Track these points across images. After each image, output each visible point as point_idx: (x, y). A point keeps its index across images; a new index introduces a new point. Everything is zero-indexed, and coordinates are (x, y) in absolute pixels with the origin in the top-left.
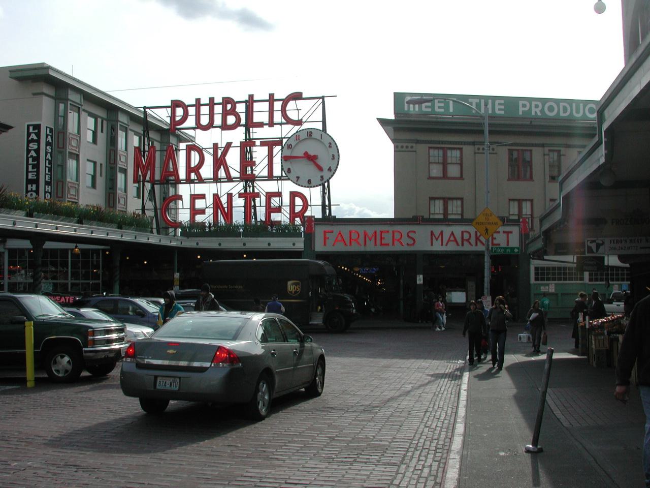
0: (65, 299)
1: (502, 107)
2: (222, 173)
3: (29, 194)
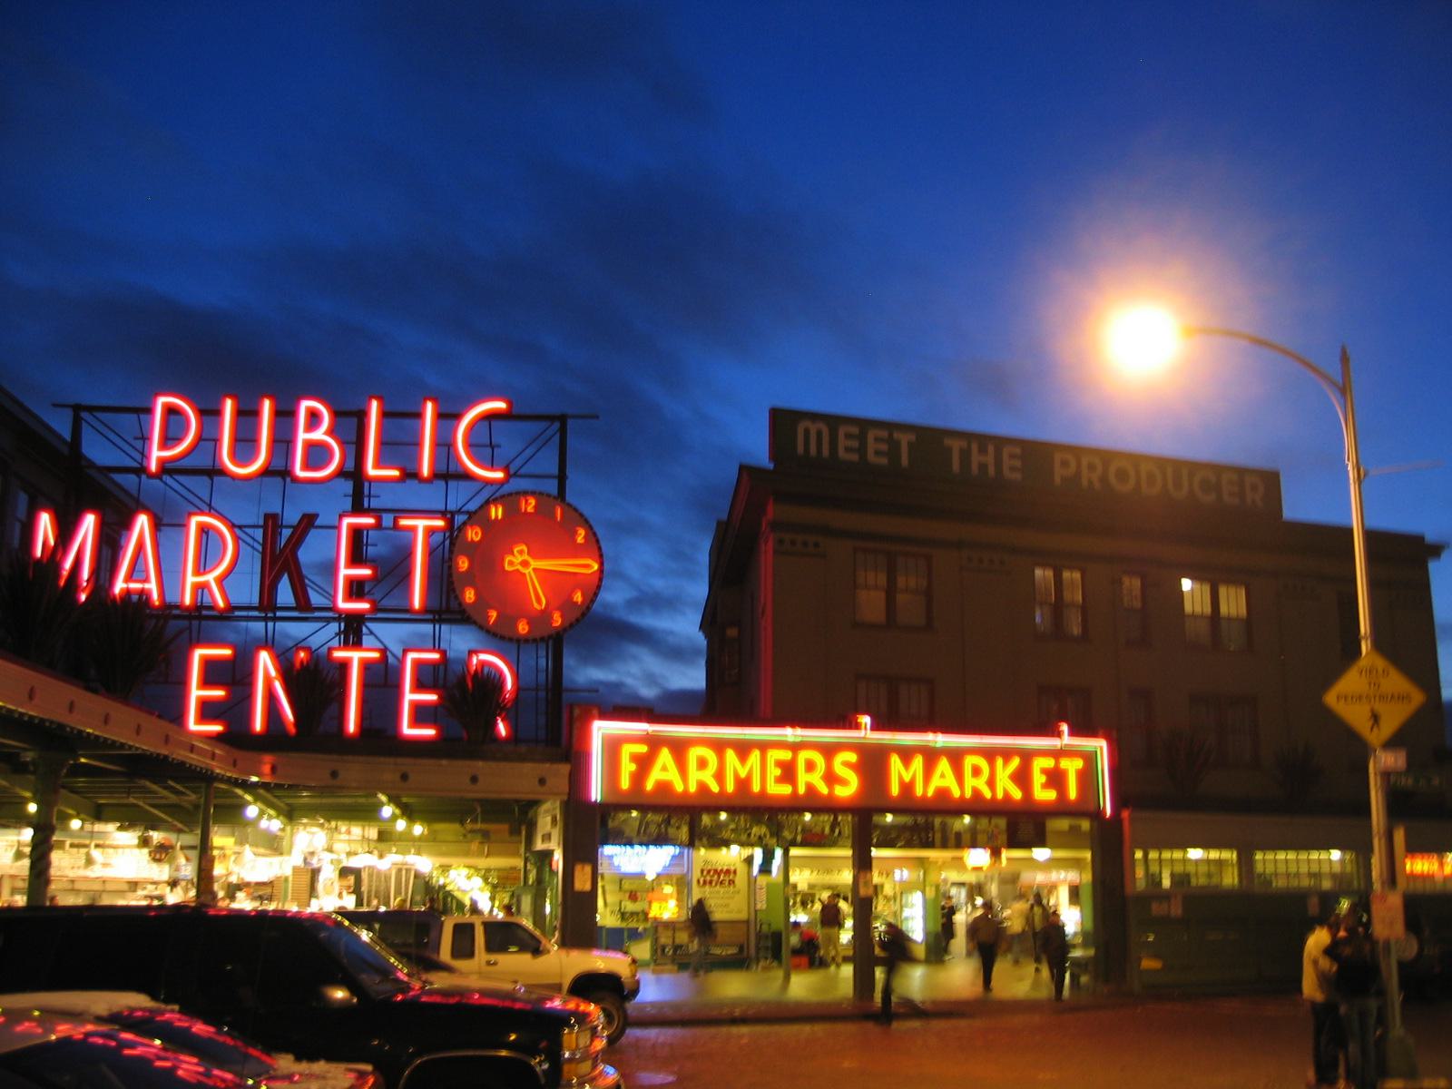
1: (1017, 463)
2: (285, 594)
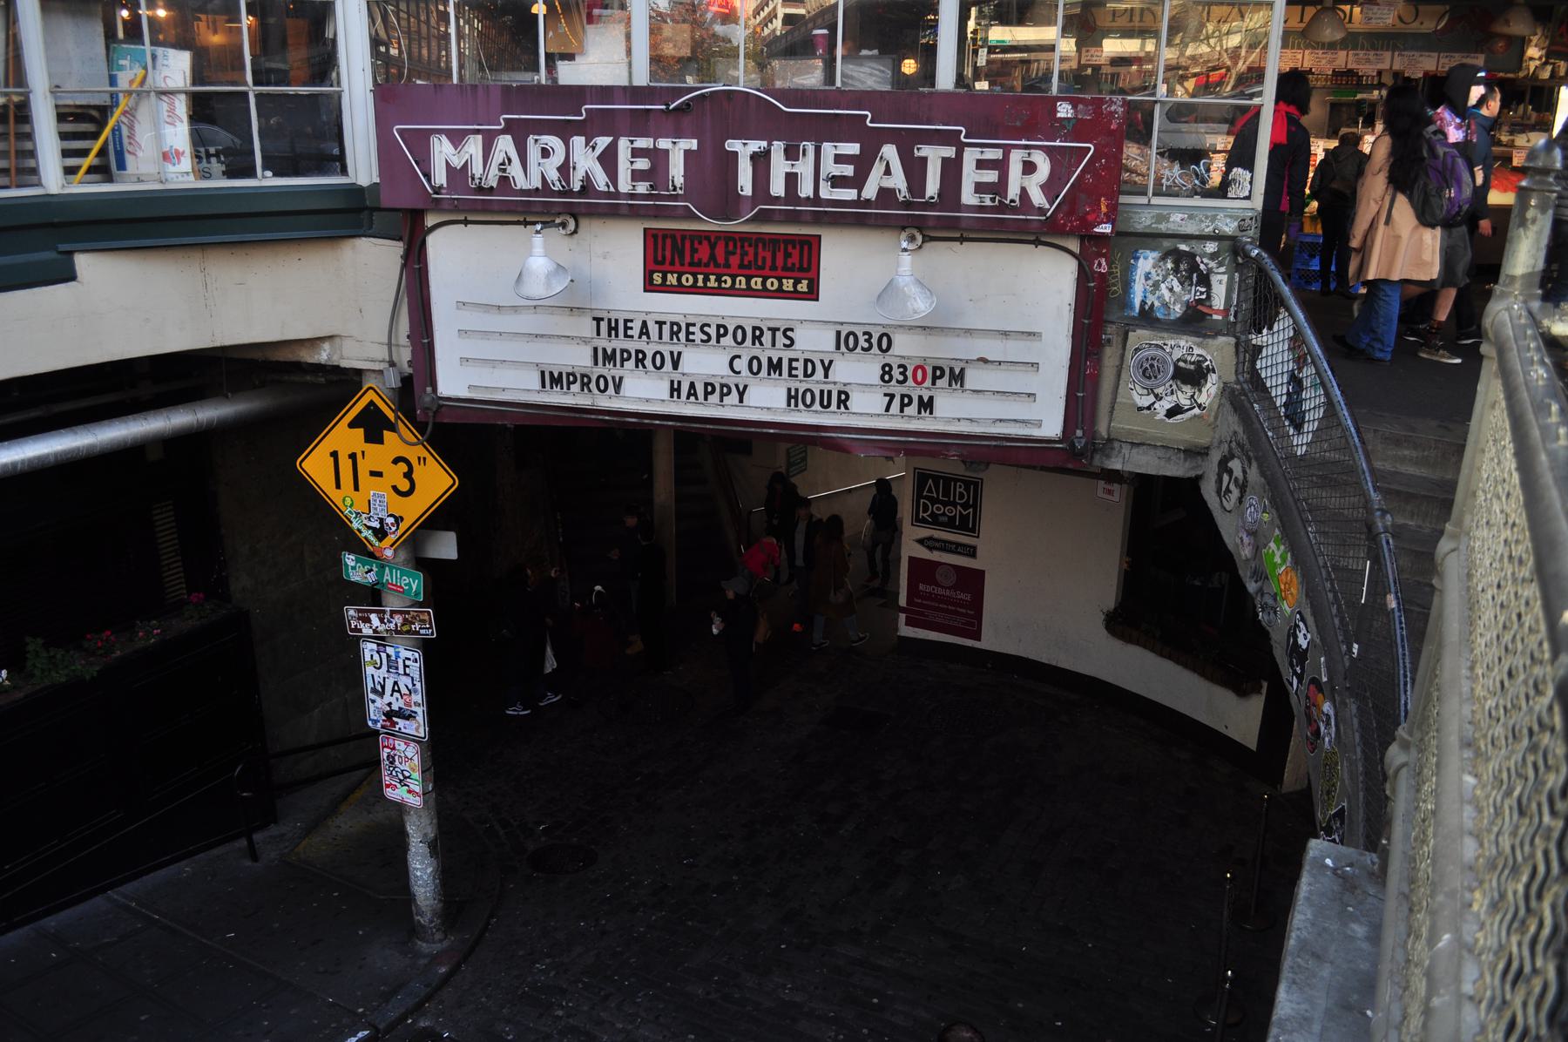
0: (915, 170)
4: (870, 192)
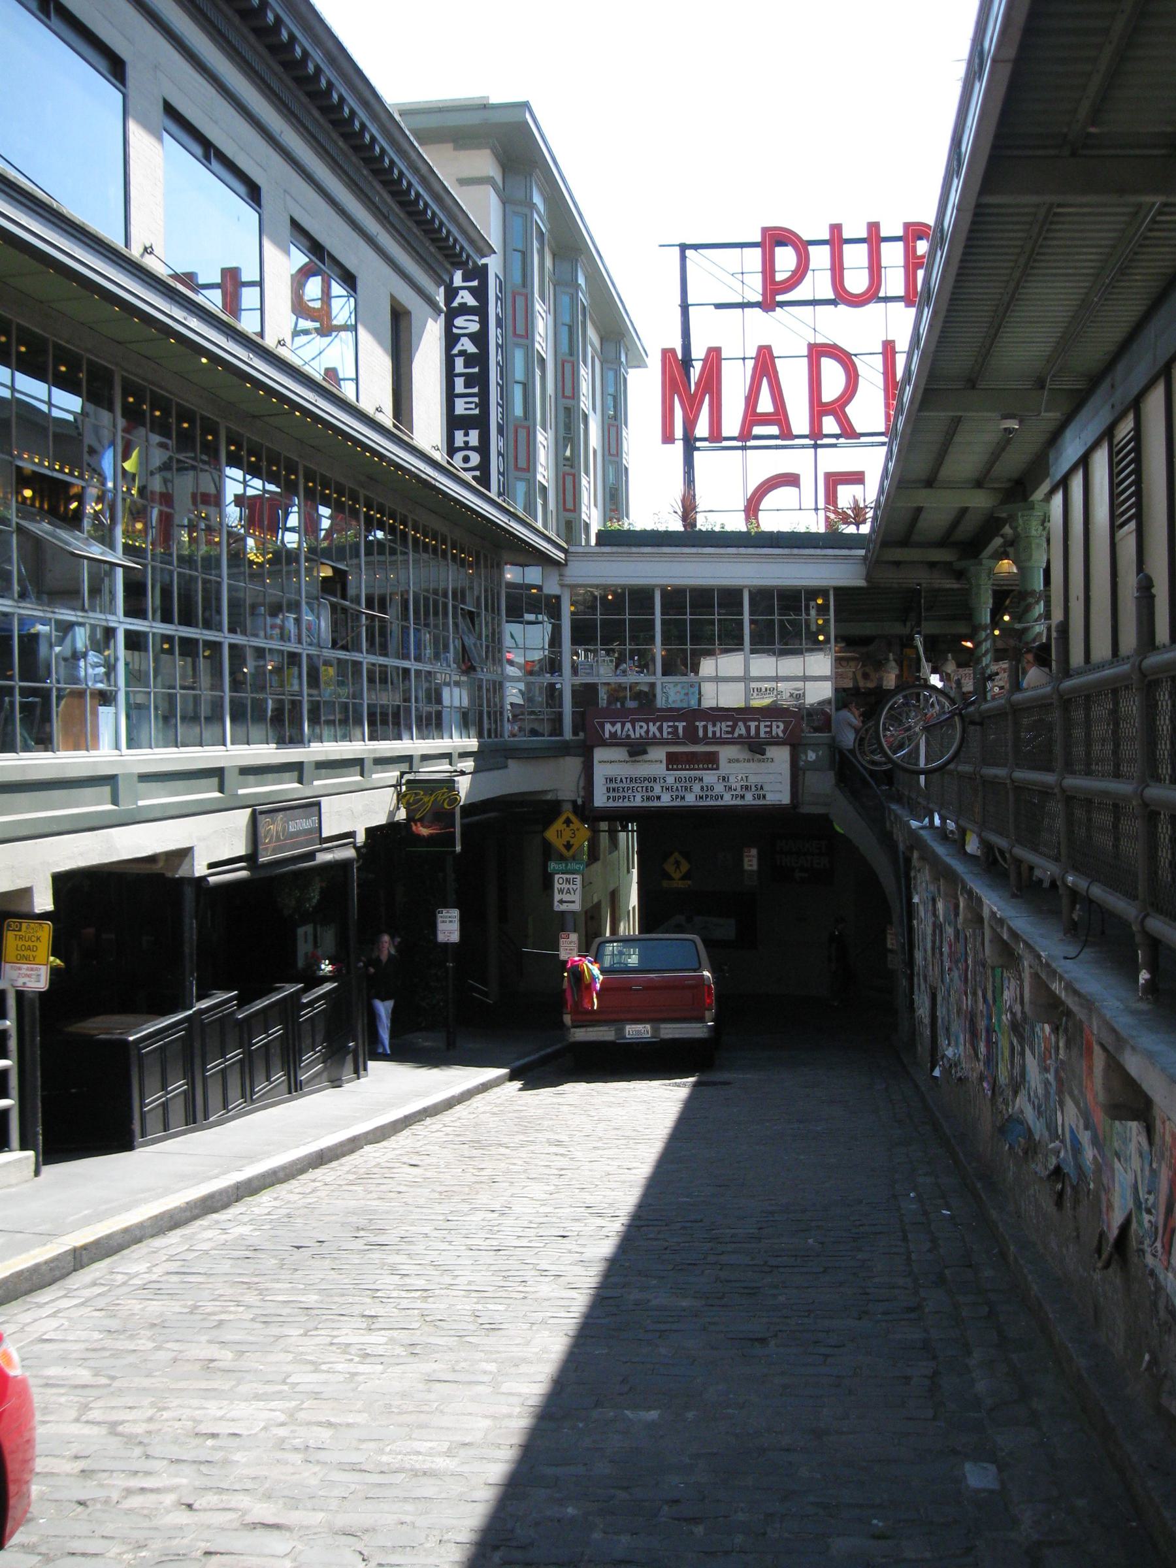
3: (459, 456)
4: (736, 735)
